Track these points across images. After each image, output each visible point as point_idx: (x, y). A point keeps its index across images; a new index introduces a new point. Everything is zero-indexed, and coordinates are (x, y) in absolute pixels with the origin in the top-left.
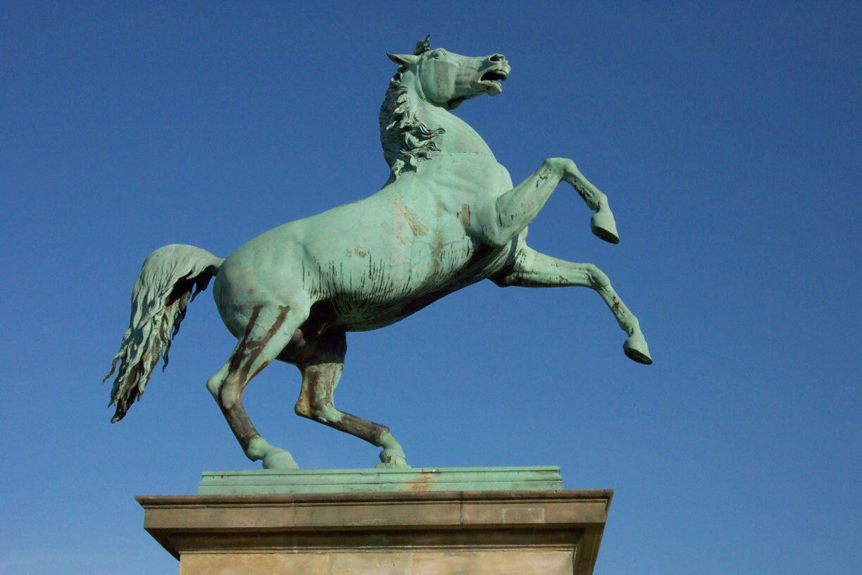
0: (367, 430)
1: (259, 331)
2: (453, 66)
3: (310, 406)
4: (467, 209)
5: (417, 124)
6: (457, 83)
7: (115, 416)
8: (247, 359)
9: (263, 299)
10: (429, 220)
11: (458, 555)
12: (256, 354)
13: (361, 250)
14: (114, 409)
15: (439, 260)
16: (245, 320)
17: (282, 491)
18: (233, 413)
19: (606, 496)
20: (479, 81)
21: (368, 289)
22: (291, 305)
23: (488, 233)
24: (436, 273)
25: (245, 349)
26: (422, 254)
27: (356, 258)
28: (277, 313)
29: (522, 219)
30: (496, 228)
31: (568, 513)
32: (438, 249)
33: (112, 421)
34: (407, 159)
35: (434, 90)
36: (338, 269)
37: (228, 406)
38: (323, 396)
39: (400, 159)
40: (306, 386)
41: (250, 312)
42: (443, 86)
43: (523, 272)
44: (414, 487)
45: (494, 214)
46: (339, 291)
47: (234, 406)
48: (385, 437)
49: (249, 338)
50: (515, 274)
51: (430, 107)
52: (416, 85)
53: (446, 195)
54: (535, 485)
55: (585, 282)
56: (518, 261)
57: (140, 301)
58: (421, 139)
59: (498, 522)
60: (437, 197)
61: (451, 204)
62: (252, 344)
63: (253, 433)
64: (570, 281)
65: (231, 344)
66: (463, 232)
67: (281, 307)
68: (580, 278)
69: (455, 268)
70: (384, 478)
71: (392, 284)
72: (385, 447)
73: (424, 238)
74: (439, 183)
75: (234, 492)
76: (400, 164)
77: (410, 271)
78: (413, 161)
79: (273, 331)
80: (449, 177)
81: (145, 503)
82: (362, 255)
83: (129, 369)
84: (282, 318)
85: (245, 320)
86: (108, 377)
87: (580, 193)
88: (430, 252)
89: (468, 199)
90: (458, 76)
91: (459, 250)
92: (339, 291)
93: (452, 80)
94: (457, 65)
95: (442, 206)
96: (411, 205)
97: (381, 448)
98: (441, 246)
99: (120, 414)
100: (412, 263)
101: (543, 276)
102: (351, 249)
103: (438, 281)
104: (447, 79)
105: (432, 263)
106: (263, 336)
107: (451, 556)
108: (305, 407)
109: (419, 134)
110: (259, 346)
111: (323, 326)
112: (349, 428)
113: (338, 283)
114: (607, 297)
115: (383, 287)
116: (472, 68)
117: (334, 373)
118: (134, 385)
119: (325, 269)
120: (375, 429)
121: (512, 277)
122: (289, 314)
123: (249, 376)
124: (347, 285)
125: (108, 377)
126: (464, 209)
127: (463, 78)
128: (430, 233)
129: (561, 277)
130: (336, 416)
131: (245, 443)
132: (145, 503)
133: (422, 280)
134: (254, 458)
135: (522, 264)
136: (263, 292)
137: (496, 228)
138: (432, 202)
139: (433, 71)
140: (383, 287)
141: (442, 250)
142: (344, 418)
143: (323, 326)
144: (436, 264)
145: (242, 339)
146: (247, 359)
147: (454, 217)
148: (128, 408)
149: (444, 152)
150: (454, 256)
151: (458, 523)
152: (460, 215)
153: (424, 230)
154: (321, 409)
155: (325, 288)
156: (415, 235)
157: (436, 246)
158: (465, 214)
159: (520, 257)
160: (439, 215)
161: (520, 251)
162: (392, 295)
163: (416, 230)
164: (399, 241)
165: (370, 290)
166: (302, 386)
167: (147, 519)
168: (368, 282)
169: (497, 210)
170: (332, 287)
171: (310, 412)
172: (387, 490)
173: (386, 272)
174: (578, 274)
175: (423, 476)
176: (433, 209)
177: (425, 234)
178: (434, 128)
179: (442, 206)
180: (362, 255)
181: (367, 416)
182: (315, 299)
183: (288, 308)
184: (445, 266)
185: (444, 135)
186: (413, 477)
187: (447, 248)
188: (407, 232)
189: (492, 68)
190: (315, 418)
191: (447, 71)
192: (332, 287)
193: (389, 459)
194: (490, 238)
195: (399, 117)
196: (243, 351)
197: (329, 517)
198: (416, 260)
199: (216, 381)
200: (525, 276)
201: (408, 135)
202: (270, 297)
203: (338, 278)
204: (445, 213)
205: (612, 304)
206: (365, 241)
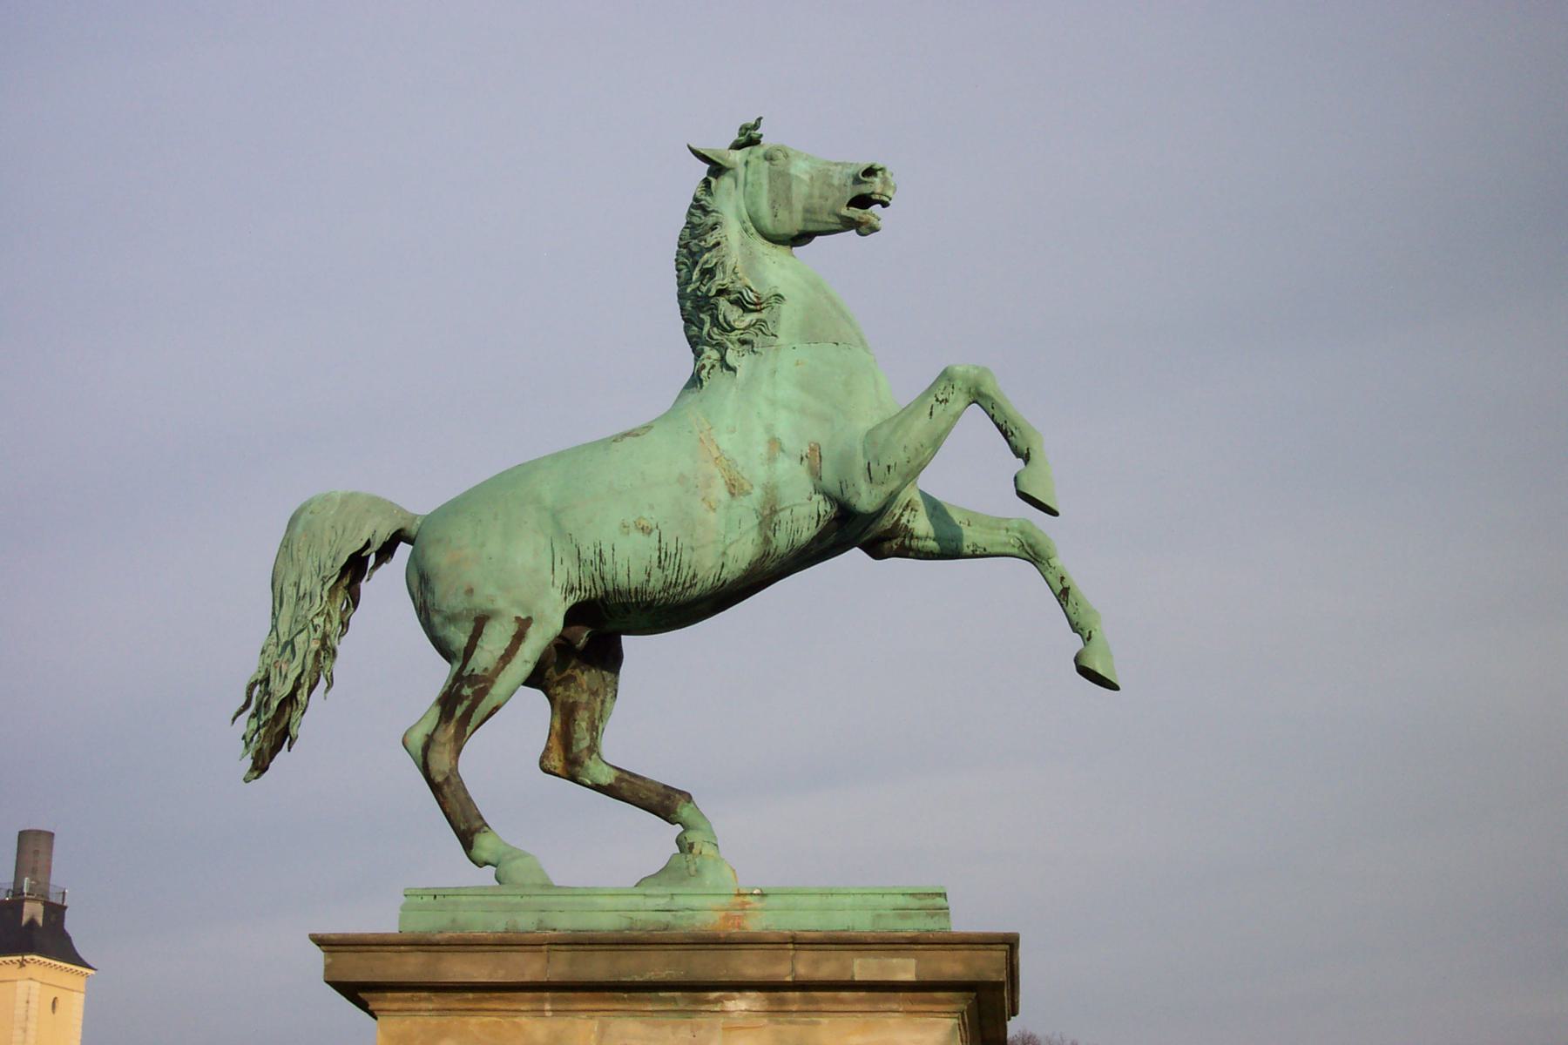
0: (656, 799)
1: (484, 657)
2: (801, 181)
3: (566, 758)
4: (816, 450)
5: (738, 285)
6: (807, 211)
7: (251, 771)
8: (466, 703)
9: (490, 606)
10: (757, 473)
11: (791, 1023)
12: (481, 694)
13: (644, 523)
14: (248, 762)
15: (770, 534)
16: (460, 639)
17: (526, 922)
18: (446, 789)
19: (1010, 943)
20: (845, 212)
21: (656, 583)
22: (534, 616)
23: (848, 494)
24: (766, 555)
25: (462, 686)
26: (745, 527)
27: (637, 536)
28: (512, 629)
29: (905, 470)
30: (863, 486)
31: (951, 966)
32: (768, 518)
33: (246, 780)
34: (721, 347)
35: (768, 222)
36: (607, 555)
37: (439, 779)
38: (585, 744)
39: (713, 346)
40: (557, 726)
41: (469, 627)
42: (783, 214)
43: (912, 537)
44: (727, 918)
45: (861, 463)
46: (610, 588)
47: (447, 780)
48: (685, 812)
49: (469, 668)
50: (899, 540)
51: (762, 247)
52: (738, 208)
53: (784, 426)
55: (1015, 551)
56: (904, 520)
57: (290, 591)
58: (746, 310)
59: (847, 978)
60: (769, 428)
62: (472, 679)
63: (478, 824)
64: (989, 550)
65: (439, 673)
66: (811, 489)
67: (518, 619)
68: (1006, 544)
69: (797, 545)
70: (680, 901)
71: (695, 576)
72: (686, 827)
73: (745, 500)
74: (773, 403)
75: (454, 921)
76: (711, 354)
77: (724, 553)
78: (731, 358)
79: (507, 656)
80: (787, 390)
81: (320, 941)
83: (275, 704)
84: (519, 638)
85: (460, 639)
86: (239, 713)
87: (999, 426)
89: (818, 434)
90: (810, 196)
91: (804, 516)
92: (610, 588)
93: (798, 206)
94: (806, 177)
95: (775, 443)
96: (725, 441)
97: (678, 828)
98: (774, 512)
99: (260, 766)
100: (728, 542)
102: (630, 521)
103: (770, 565)
104: (789, 202)
105: (759, 540)
106: (491, 666)
107: (778, 1023)
108: (556, 762)
109: (740, 303)
110: (482, 685)
112: (627, 794)
113: (608, 577)
114: (1050, 577)
115: (680, 581)
116: (831, 185)
117: (603, 702)
118: (282, 725)
119: (588, 554)
120: (668, 797)
121: (894, 544)
123: (469, 729)
124: (622, 580)
125: (239, 713)
126: (812, 450)
127: (816, 201)
128: (757, 492)
130: (606, 777)
131: (467, 840)
132: (320, 941)
133: (744, 565)
134: (481, 864)
135: (910, 525)
136: (490, 595)
137: (863, 486)
138: (760, 436)
139: (766, 187)
140: (680, 581)
141: (776, 519)
142: (618, 779)
144: (767, 541)
145: (457, 666)
146: (466, 703)
147: (796, 463)
148: (272, 758)
149: (782, 340)
150: (795, 527)
151: (789, 979)
152: (806, 462)
153: (747, 487)
154: (581, 764)
155: (587, 584)
156: (733, 495)
157: (767, 512)
158: (813, 459)
159: (907, 514)
160: (772, 459)
162: (695, 591)
163: (734, 489)
164: (705, 506)
165: (659, 586)
166: (552, 726)
167: (328, 968)
168: (657, 574)
169: (865, 455)
170: (599, 582)
171: (564, 768)
172: (684, 923)
173: (685, 558)
174: (1005, 539)
175: (740, 899)
176: (762, 449)
177: (749, 493)
178: (765, 292)
179: (775, 443)
181: (657, 770)
182: (571, 600)
184: (781, 542)
185: (785, 309)
186: (724, 900)
187: (784, 516)
188: (720, 492)
189: (865, 189)
190: (573, 779)
191: (789, 187)
192: (599, 582)
193: (691, 846)
194: (853, 501)
195: (708, 273)
196: (459, 690)
197: (598, 967)
198: (734, 536)
199: (418, 739)
200: (915, 543)
201: (723, 304)
202: (501, 603)
203: (607, 568)
205: (1059, 588)
206: (652, 507)
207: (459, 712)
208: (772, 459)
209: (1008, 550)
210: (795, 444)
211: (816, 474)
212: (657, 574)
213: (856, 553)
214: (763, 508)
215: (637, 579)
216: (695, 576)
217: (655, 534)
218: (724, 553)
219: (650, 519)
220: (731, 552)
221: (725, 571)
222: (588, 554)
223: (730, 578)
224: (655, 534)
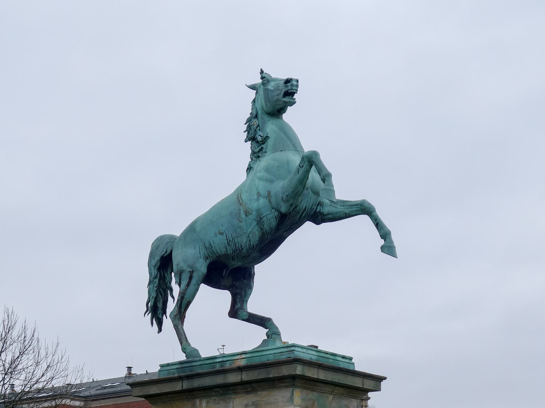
15: (262, 226)
24: (263, 234)
27: (219, 236)
32: (260, 221)
36: (212, 245)
54: (283, 355)
56: (318, 210)
61: (262, 193)
64: (351, 214)
67: (189, 271)
73: (251, 217)
77: (248, 236)
82: (221, 234)
84: (191, 278)
88: (256, 223)
95: (259, 194)
98: (261, 219)
101: (335, 215)
111: (225, 271)
119: (207, 245)
122: (195, 274)
123: (183, 310)
126: (268, 193)
128: (254, 213)
129: (345, 213)
135: (321, 211)
143: (225, 271)
144: (262, 229)
155: (211, 255)
156: (246, 216)
159: (319, 208)
161: (318, 204)
163: (247, 214)
173: (236, 240)
174: (355, 209)
176: (255, 197)
179: (259, 194)
180: (221, 234)
182: (208, 262)
183: (193, 272)
184: (266, 227)
202: (185, 267)
203: (214, 249)
204: (261, 198)
206: (222, 225)
207: (171, 305)
208: (258, 200)
209: (358, 213)
210: (263, 192)
212: (228, 247)
213: (308, 225)
214: (257, 218)
215: (223, 251)
216: (241, 246)
217: (224, 234)
218: (248, 236)
220: (250, 235)
221: (251, 242)
222: (207, 245)
223: (255, 244)
224: (224, 234)
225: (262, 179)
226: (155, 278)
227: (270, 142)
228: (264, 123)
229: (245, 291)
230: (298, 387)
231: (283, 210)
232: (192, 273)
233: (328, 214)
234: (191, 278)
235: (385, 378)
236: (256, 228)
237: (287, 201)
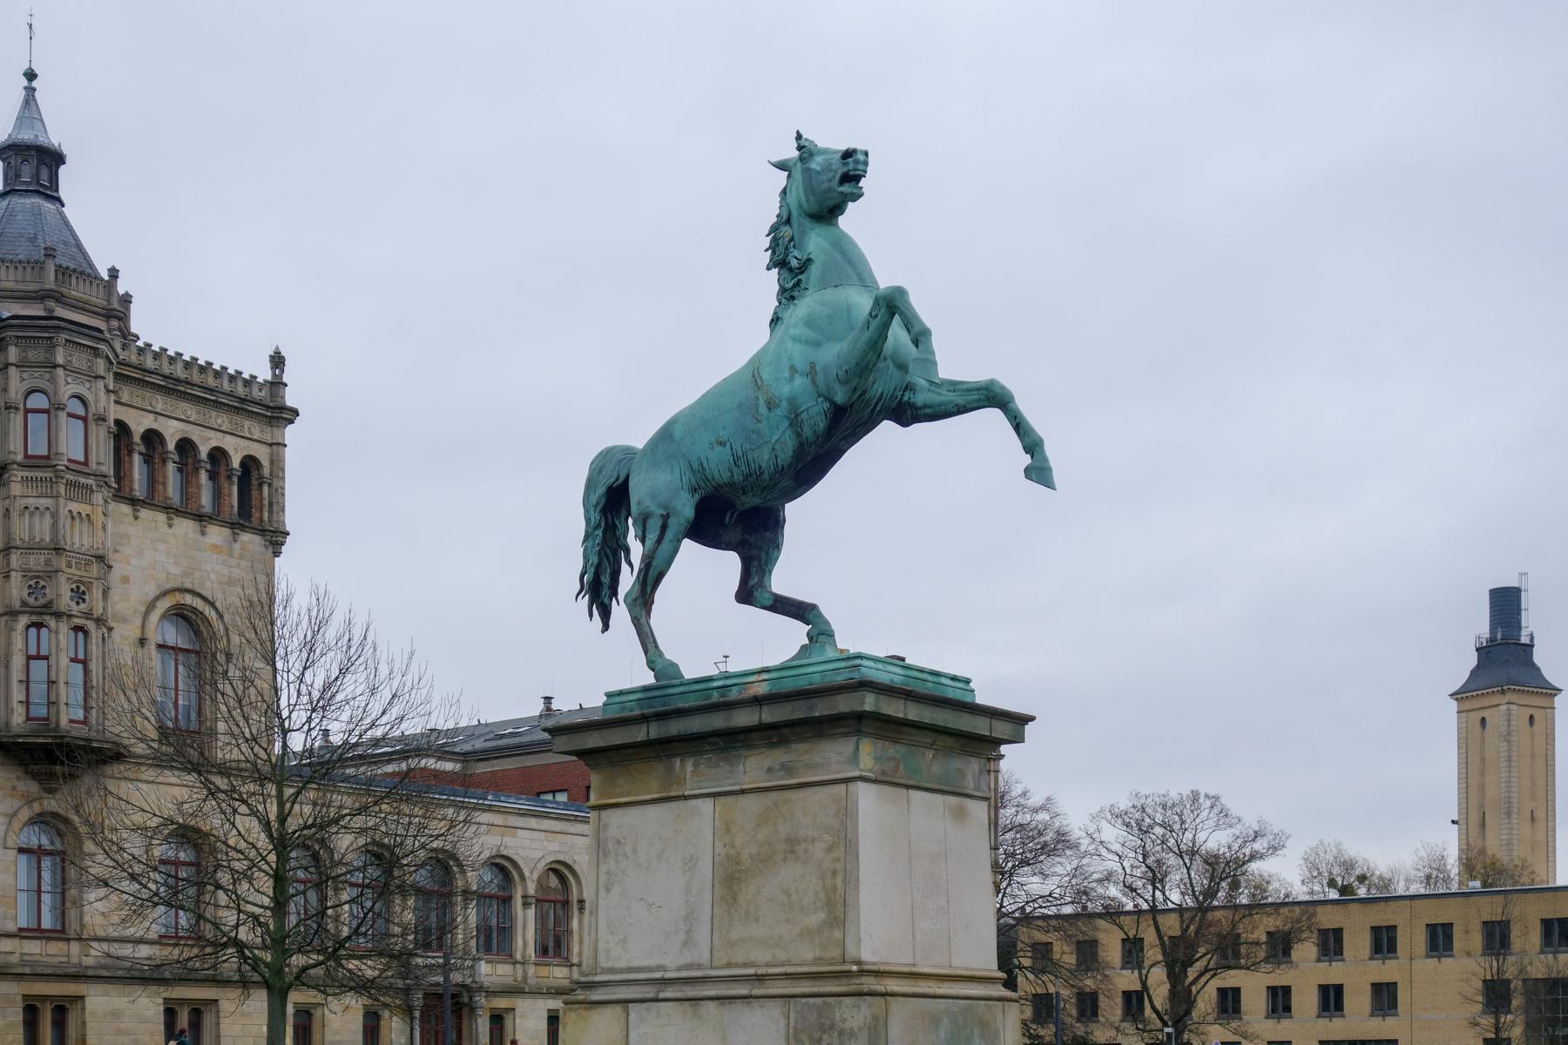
4: (813, 366)
24: (801, 444)
27: (719, 448)
28: (660, 522)
32: (795, 420)
60: (790, 359)
61: (799, 366)
73: (778, 412)
82: (722, 444)
84: (664, 528)
95: (793, 369)
98: (797, 415)
119: (696, 466)
122: (672, 521)
128: (784, 404)
144: (798, 435)
159: (907, 395)
163: (771, 405)
176: (787, 374)
179: (793, 369)
182: (697, 497)
184: (807, 432)
202: (653, 508)
207: (627, 580)
208: (791, 379)
210: (801, 365)
211: (814, 382)
212: (735, 469)
213: (887, 427)
215: (726, 476)
219: (724, 435)
222: (696, 466)
225: (800, 341)
226: (596, 528)
227: (814, 270)
228: (803, 234)
229: (767, 553)
230: (868, 735)
231: (840, 397)
232: (666, 518)
233: (925, 406)
234: (664, 528)
235: (1032, 719)
236: (789, 433)
237: (847, 382)
